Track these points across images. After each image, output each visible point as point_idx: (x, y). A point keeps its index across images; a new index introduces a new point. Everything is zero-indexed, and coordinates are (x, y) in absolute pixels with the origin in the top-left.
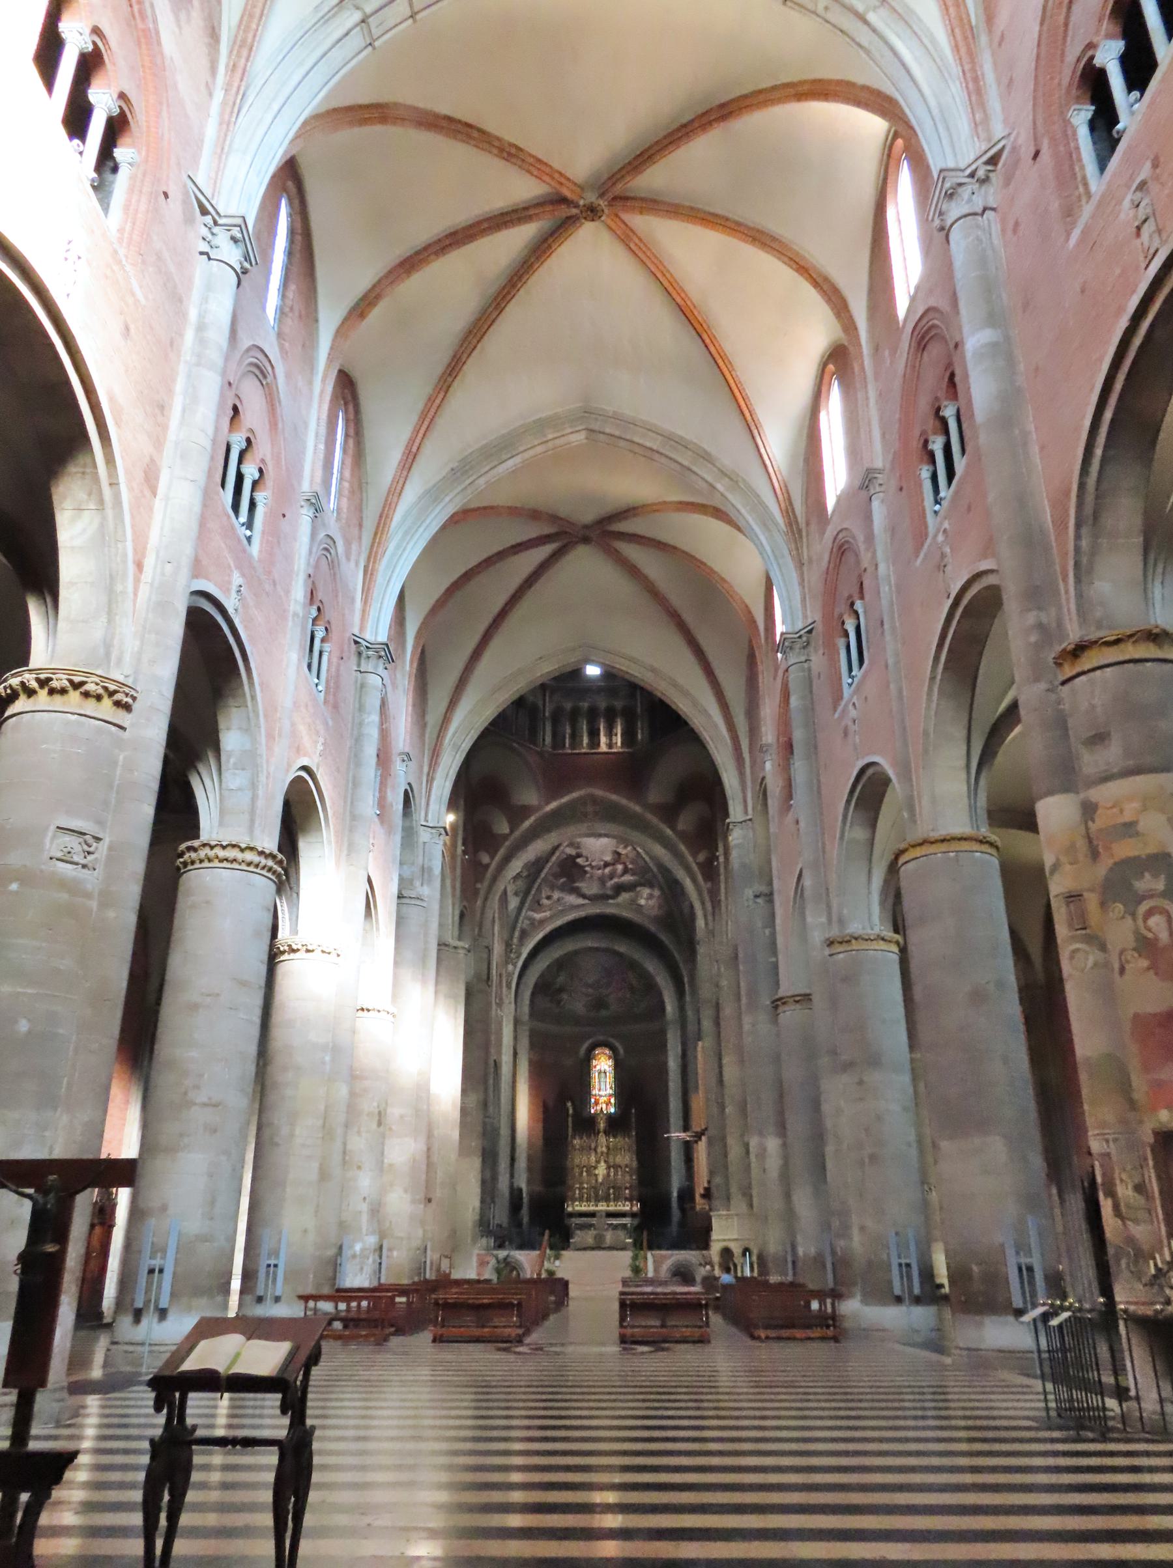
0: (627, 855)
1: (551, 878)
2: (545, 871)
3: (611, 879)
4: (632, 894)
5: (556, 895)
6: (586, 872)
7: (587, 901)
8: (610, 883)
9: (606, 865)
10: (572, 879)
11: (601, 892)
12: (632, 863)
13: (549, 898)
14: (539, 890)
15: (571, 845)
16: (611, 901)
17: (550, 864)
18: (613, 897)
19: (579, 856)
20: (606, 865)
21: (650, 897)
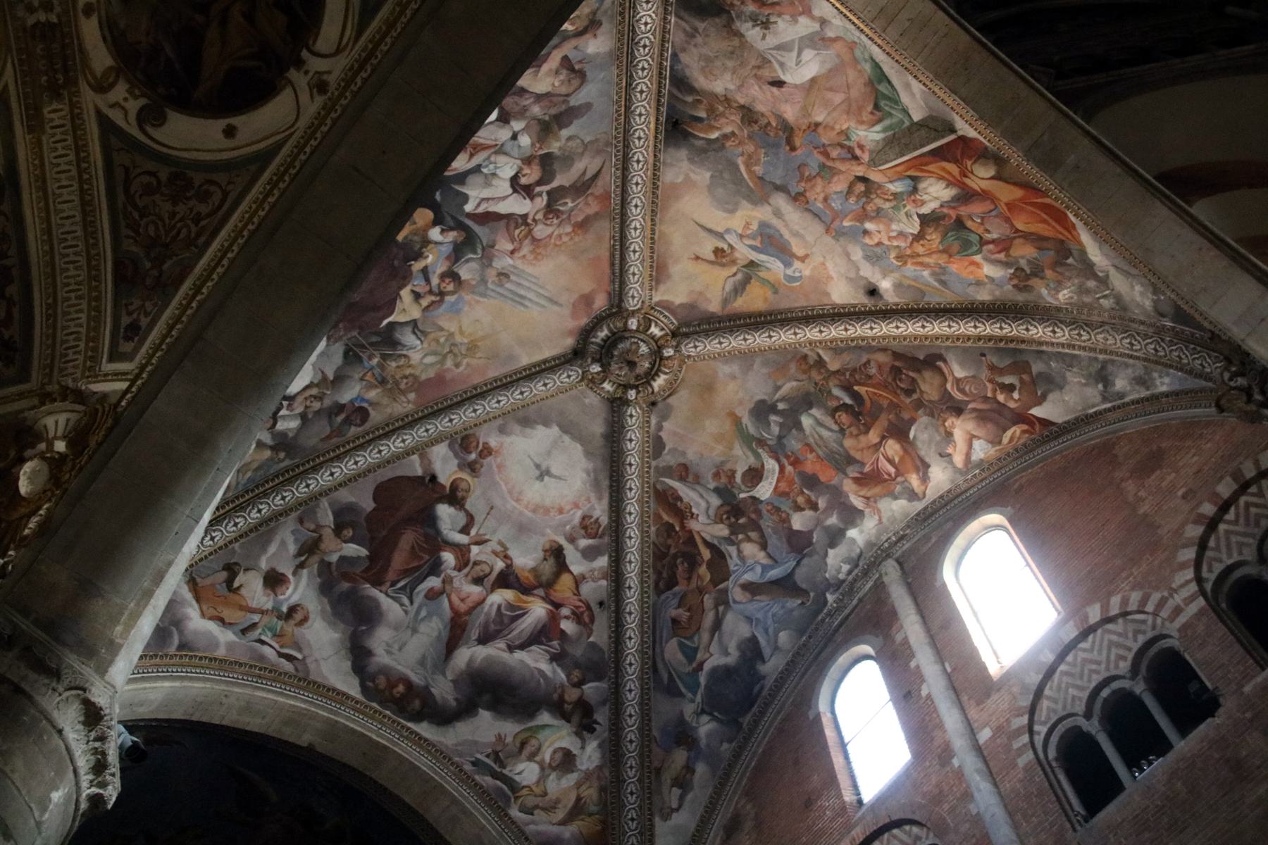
0: (578, 581)
1: (327, 518)
2: (346, 468)
3: (484, 640)
4: (510, 729)
5: (300, 590)
6: (435, 568)
7: (352, 687)
8: (469, 655)
9: (506, 579)
10: (376, 571)
11: (416, 679)
12: (577, 617)
13: (274, 581)
14: (263, 532)
15: (464, 443)
16: (425, 729)
17: (368, 458)
18: (444, 717)
19: (454, 497)
20: (506, 579)
21: (566, 761)
